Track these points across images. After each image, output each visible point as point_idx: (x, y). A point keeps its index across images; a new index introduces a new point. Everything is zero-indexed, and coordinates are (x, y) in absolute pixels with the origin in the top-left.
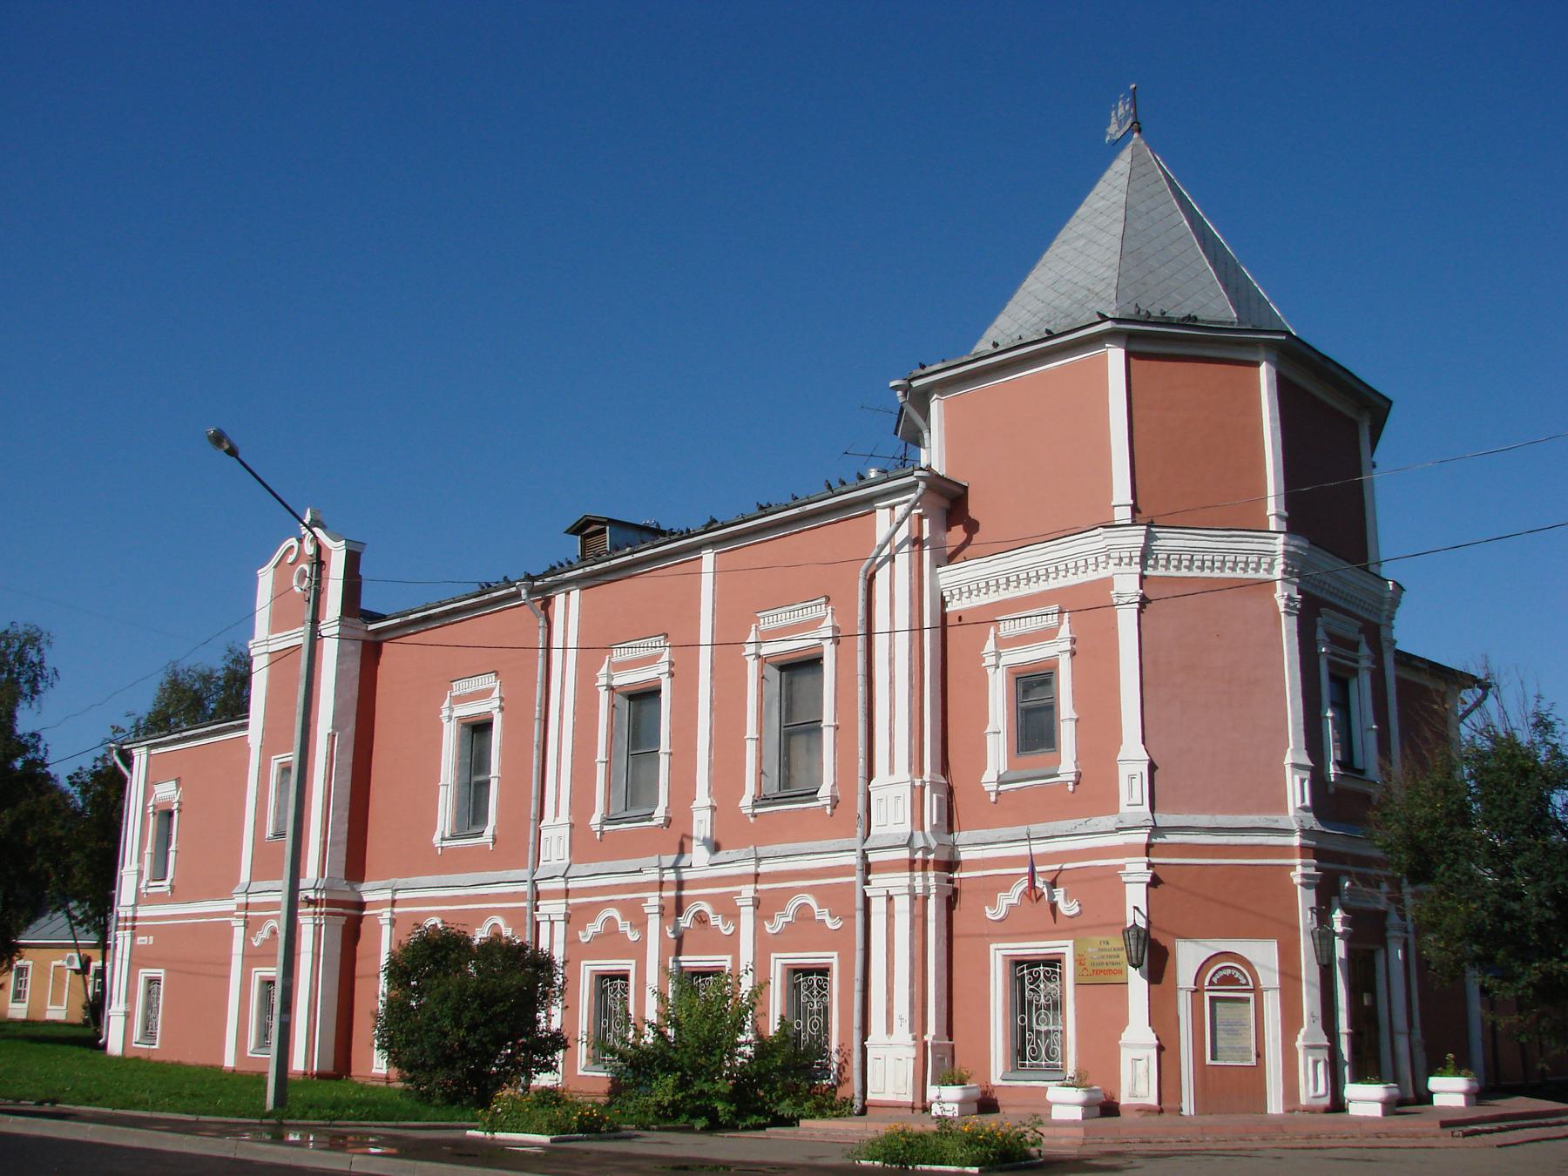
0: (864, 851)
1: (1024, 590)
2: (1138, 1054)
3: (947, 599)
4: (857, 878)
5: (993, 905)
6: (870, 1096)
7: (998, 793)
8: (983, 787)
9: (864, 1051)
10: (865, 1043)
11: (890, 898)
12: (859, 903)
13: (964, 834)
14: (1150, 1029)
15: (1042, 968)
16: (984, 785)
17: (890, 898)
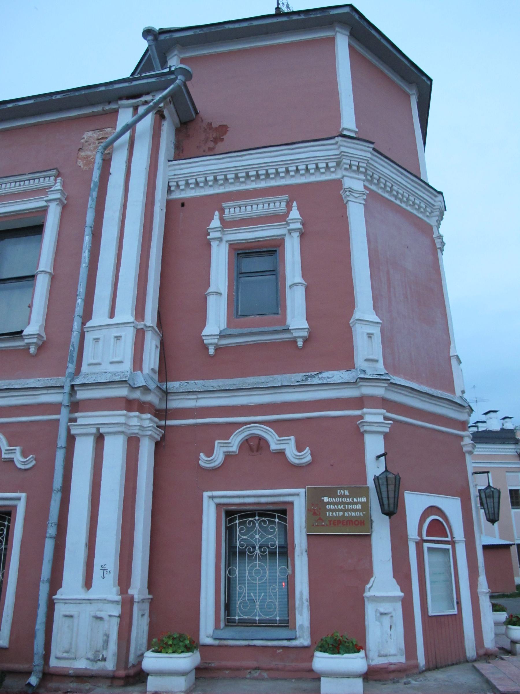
0: (73, 386)
1: (252, 186)
2: (384, 607)
3: (172, 188)
4: (63, 416)
5: (210, 453)
6: (53, 663)
7: (218, 349)
8: (203, 340)
9: (51, 605)
10: (54, 597)
11: (100, 438)
12: (62, 441)
13: (176, 384)
14: (394, 581)
15: (257, 518)
16: (204, 338)
17: (100, 438)
